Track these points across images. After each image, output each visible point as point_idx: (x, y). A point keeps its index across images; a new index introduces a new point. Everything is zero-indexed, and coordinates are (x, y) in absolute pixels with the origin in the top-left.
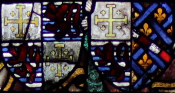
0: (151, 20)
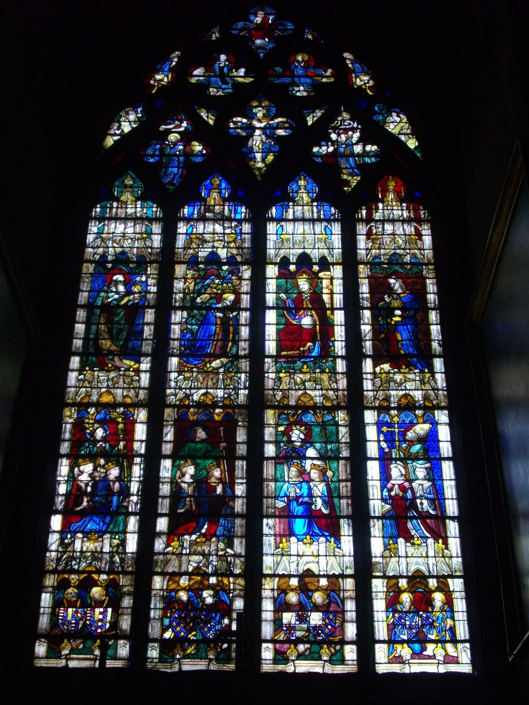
0: (328, 618)
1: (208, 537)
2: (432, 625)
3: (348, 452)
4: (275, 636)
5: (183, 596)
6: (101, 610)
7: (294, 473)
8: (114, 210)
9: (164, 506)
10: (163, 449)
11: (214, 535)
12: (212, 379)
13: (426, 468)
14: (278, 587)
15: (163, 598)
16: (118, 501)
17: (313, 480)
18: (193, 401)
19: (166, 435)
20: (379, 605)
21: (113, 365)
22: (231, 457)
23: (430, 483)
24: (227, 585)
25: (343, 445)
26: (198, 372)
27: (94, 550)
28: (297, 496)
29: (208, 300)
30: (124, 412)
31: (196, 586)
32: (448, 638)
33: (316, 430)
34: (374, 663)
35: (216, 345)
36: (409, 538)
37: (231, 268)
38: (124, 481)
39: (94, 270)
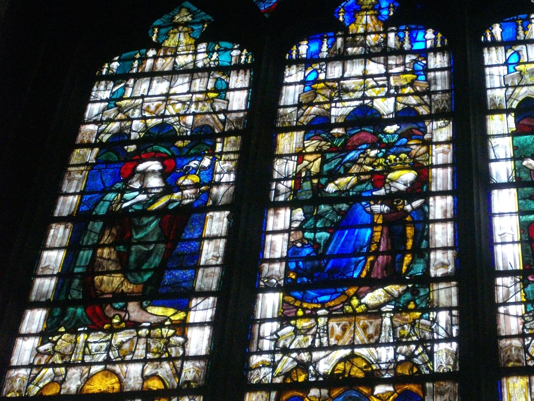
8: (149, 62)
12: (365, 328)
18: (317, 374)
21: (122, 320)
26: (330, 316)
29: (353, 187)
35: (372, 263)
37: (404, 128)
39: (96, 158)
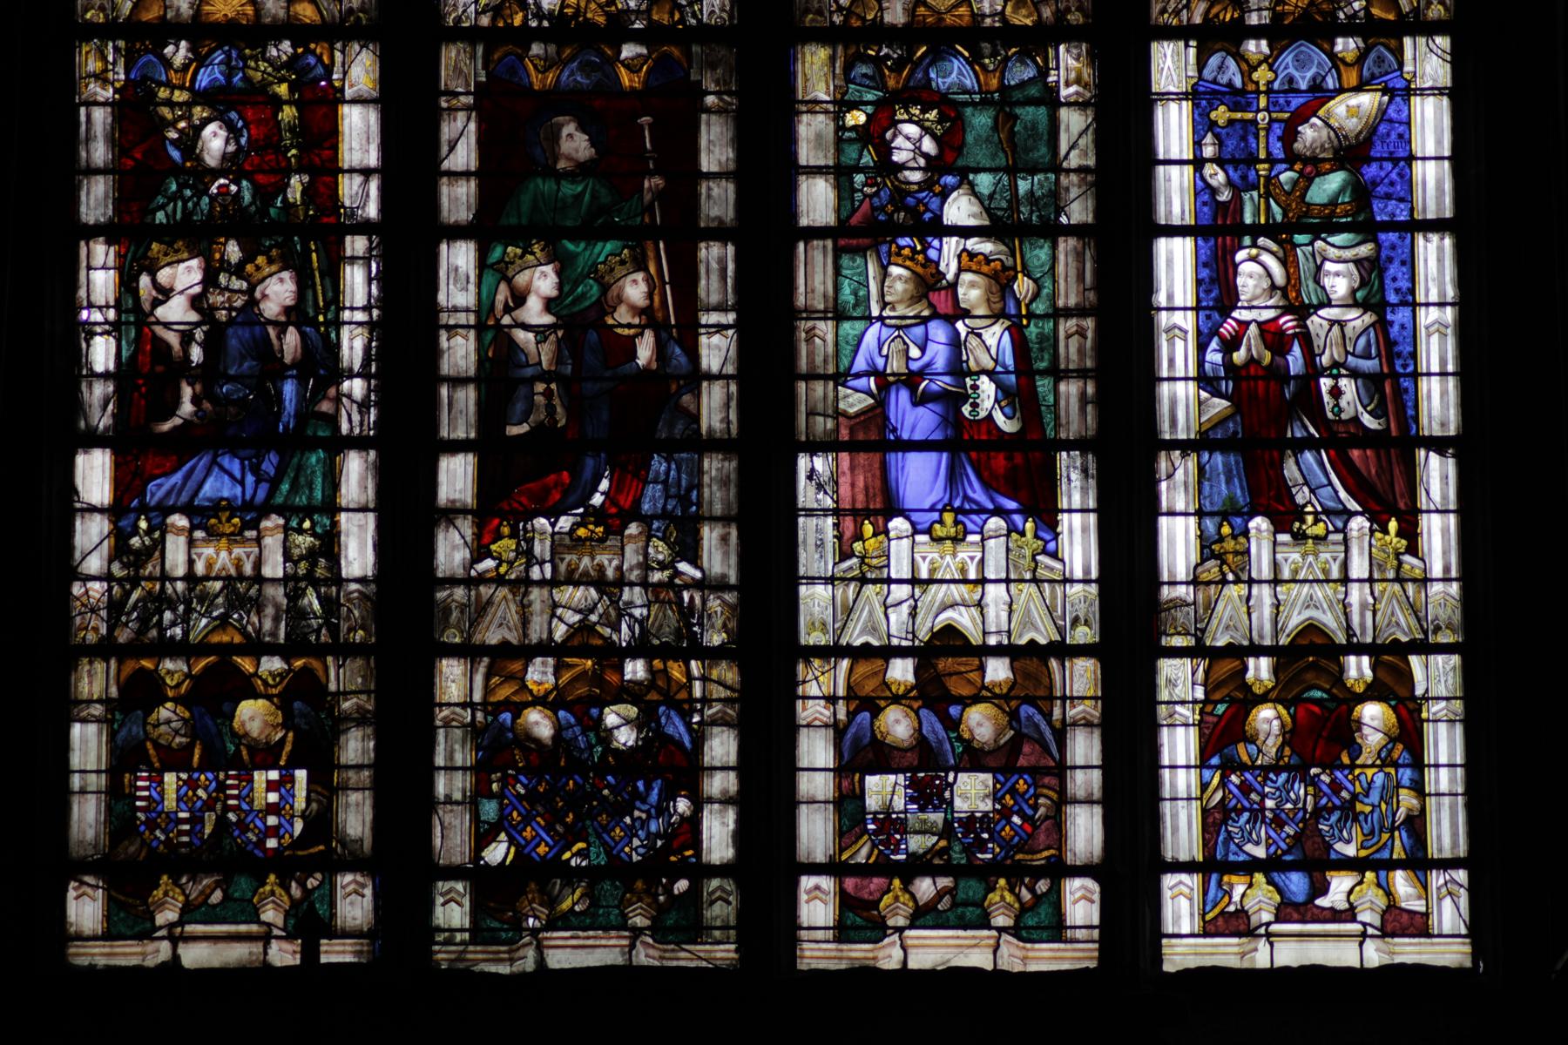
0: (1013, 791)
1: (612, 521)
2: (1349, 812)
3: (1090, 204)
4: (841, 851)
5: (539, 723)
6: (274, 775)
7: (899, 286)
9: (459, 413)
10: (445, 201)
11: (635, 514)
13: (1358, 262)
14: (849, 687)
15: (474, 732)
16: (301, 396)
17: (965, 314)
18: (540, 14)
19: (452, 148)
20: (1179, 745)
22: (682, 232)
23: (1369, 318)
24: (681, 687)
25: (1074, 178)
27: (233, 572)
28: (911, 373)
30: (294, 58)
31: (582, 690)
32: (1399, 853)
33: (980, 121)
34: (1157, 934)
36: (1286, 517)
38: (316, 325)
